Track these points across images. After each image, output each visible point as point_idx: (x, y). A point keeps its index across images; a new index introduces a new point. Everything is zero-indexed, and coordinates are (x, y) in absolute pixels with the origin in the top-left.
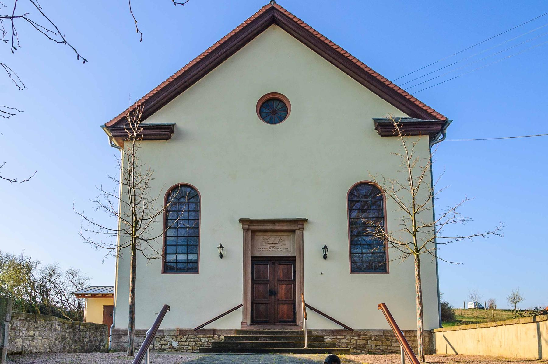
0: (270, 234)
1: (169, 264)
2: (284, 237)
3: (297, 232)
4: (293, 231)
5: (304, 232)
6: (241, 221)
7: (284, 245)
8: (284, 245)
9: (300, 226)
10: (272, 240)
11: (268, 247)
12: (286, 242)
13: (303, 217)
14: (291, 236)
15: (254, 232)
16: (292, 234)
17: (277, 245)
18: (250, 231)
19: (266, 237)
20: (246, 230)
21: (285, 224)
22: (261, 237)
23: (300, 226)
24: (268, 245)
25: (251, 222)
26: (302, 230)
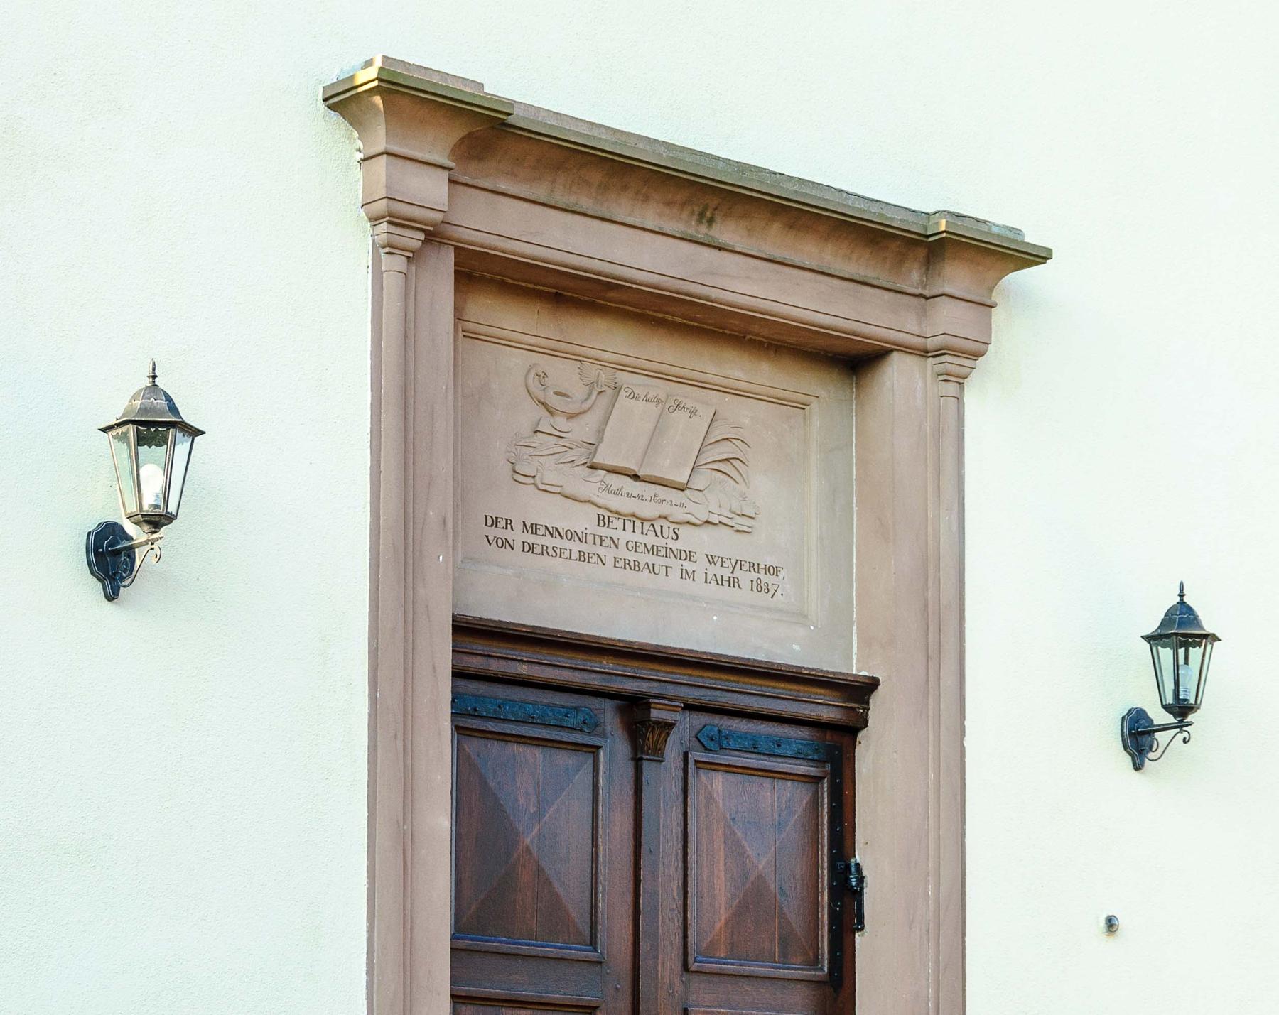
0: (610, 340)
1: (802, 769)
2: (745, 414)
3: (899, 376)
4: (854, 361)
5: (970, 399)
6: (400, 102)
7: (739, 523)
8: (739, 523)
9: (948, 320)
10: (629, 427)
11: (583, 520)
12: (763, 488)
13: (1033, 237)
14: (817, 417)
15: (482, 273)
16: (819, 388)
17: (672, 503)
18: (446, 262)
19: (563, 374)
20: (413, 237)
21: (810, 251)
22: (516, 362)
23: (948, 320)
24: (591, 486)
25: (487, 135)
26: (957, 358)
